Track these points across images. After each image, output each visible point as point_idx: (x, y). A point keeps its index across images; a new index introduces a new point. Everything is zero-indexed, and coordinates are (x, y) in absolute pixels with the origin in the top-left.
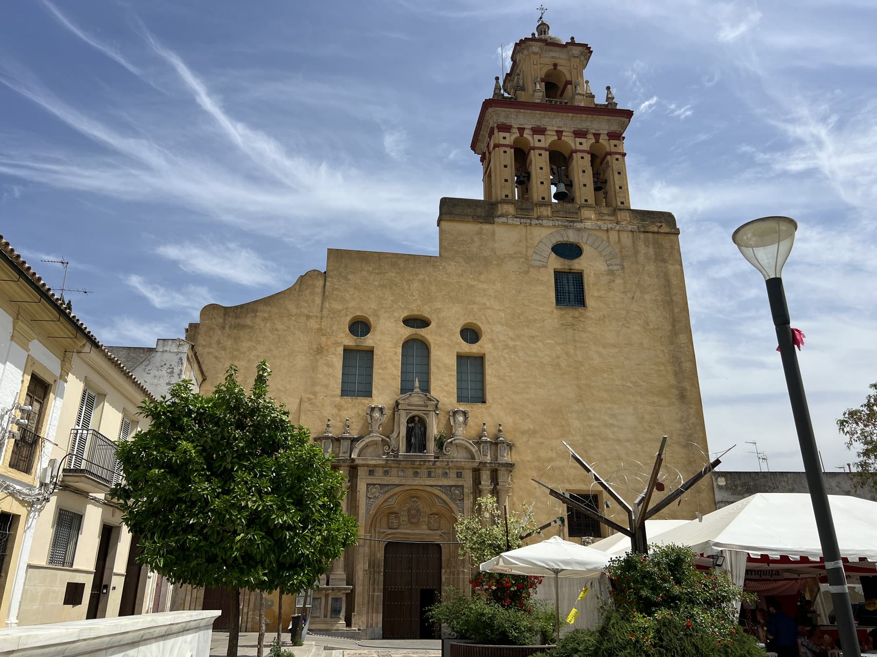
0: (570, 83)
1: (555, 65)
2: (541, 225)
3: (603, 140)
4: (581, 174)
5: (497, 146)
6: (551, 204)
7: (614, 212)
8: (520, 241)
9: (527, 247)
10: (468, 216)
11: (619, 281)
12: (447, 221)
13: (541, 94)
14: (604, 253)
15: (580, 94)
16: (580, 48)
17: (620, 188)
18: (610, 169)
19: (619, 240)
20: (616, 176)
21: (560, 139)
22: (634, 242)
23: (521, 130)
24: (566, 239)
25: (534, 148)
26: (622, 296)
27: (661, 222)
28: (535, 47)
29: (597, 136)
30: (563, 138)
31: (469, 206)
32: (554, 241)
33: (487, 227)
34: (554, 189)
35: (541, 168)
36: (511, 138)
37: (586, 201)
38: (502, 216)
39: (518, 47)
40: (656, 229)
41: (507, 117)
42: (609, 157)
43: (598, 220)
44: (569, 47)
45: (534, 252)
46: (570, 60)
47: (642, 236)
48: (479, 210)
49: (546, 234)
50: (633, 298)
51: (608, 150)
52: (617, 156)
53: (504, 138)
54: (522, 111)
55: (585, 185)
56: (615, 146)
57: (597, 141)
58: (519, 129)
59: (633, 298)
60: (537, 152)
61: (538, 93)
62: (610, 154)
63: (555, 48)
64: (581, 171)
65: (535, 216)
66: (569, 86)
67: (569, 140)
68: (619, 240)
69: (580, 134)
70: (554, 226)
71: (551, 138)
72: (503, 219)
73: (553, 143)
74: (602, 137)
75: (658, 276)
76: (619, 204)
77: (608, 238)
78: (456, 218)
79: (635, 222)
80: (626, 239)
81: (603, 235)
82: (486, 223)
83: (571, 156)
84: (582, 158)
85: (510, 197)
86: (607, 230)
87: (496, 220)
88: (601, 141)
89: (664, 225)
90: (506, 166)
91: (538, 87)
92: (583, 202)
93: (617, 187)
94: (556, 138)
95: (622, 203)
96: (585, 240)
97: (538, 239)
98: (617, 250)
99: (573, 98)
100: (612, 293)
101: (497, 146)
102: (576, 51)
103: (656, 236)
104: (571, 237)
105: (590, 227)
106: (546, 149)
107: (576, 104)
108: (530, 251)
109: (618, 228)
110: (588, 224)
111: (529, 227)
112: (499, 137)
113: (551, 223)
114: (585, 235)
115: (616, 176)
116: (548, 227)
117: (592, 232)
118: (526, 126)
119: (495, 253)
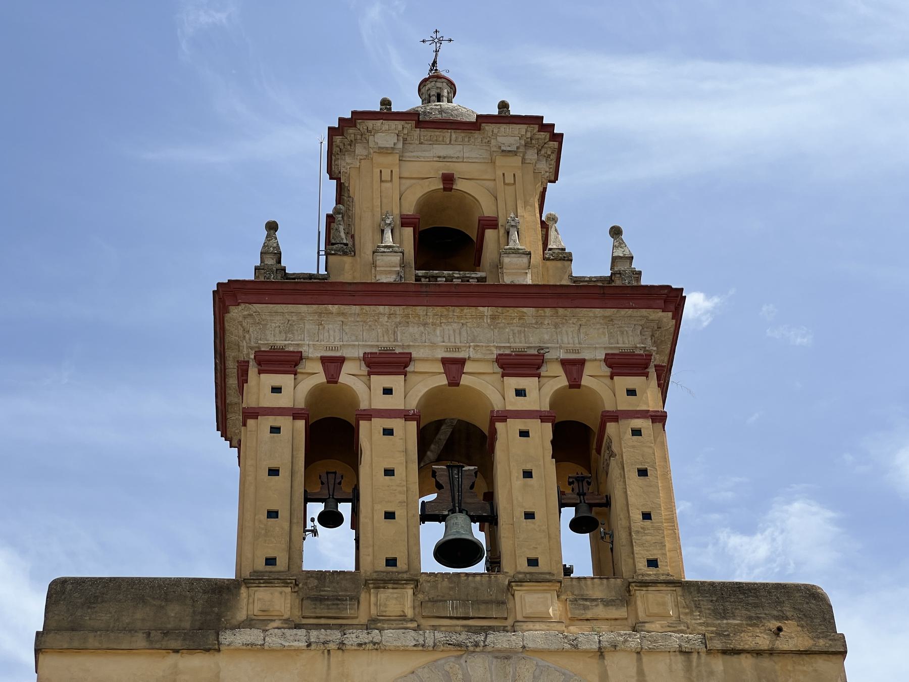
0: (492, 223)
1: (448, 180)
3: (595, 379)
4: (518, 481)
5: (252, 413)
6: (415, 580)
7: (625, 598)
10: (131, 630)
12: (61, 651)
13: (396, 259)
15: (516, 252)
16: (522, 129)
17: (647, 516)
18: (613, 462)
21: (454, 382)
23: (332, 365)
25: (369, 415)
27: (783, 618)
29: (574, 367)
30: (465, 380)
31: (141, 600)
34: (432, 534)
35: (389, 472)
36: (295, 390)
37: (533, 562)
38: (249, 623)
39: (338, 139)
40: (763, 641)
41: (289, 329)
42: (611, 428)
43: (572, 619)
44: (488, 128)
46: (493, 162)
47: (718, 664)
48: (173, 610)
51: (609, 407)
52: (637, 423)
53: (276, 390)
55: (529, 516)
56: (631, 392)
57: (575, 384)
58: (324, 360)
60: (379, 424)
61: (389, 255)
62: (615, 417)
63: (447, 134)
64: (517, 474)
65: (363, 619)
66: (489, 234)
67: (488, 388)
70: (422, 647)
71: (425, 380)
72: (252, 635)
73: (432, 397)
74: (588, 370)
76: (642, 566)
78: (92, 642)
79: (696, 620)
81: (588, 669)
82: (191, 650)
83: (493, 432)
84: (524, 434)
85: (282, 564)
86: (601, 653)
87: (227, 637)
88: (586, 381)
89: (790, 627)
90: (274, 472)
91: (388, 239)
92: (523, 566)
93: (637, 516)
94: (443, 381)
95: (653, 563)
99: (498, 266)
101: (252, 413)
102: (508, 137)
103: (766, 663)
105: (540, 644)
106: (407, 416)
107: (507, 280)
109: (634, 642)
110: (534, 636)
111: (336, 657)
112: (260, 388)
113: (410, 638)
115: (634, 482)
116: (405, 650)
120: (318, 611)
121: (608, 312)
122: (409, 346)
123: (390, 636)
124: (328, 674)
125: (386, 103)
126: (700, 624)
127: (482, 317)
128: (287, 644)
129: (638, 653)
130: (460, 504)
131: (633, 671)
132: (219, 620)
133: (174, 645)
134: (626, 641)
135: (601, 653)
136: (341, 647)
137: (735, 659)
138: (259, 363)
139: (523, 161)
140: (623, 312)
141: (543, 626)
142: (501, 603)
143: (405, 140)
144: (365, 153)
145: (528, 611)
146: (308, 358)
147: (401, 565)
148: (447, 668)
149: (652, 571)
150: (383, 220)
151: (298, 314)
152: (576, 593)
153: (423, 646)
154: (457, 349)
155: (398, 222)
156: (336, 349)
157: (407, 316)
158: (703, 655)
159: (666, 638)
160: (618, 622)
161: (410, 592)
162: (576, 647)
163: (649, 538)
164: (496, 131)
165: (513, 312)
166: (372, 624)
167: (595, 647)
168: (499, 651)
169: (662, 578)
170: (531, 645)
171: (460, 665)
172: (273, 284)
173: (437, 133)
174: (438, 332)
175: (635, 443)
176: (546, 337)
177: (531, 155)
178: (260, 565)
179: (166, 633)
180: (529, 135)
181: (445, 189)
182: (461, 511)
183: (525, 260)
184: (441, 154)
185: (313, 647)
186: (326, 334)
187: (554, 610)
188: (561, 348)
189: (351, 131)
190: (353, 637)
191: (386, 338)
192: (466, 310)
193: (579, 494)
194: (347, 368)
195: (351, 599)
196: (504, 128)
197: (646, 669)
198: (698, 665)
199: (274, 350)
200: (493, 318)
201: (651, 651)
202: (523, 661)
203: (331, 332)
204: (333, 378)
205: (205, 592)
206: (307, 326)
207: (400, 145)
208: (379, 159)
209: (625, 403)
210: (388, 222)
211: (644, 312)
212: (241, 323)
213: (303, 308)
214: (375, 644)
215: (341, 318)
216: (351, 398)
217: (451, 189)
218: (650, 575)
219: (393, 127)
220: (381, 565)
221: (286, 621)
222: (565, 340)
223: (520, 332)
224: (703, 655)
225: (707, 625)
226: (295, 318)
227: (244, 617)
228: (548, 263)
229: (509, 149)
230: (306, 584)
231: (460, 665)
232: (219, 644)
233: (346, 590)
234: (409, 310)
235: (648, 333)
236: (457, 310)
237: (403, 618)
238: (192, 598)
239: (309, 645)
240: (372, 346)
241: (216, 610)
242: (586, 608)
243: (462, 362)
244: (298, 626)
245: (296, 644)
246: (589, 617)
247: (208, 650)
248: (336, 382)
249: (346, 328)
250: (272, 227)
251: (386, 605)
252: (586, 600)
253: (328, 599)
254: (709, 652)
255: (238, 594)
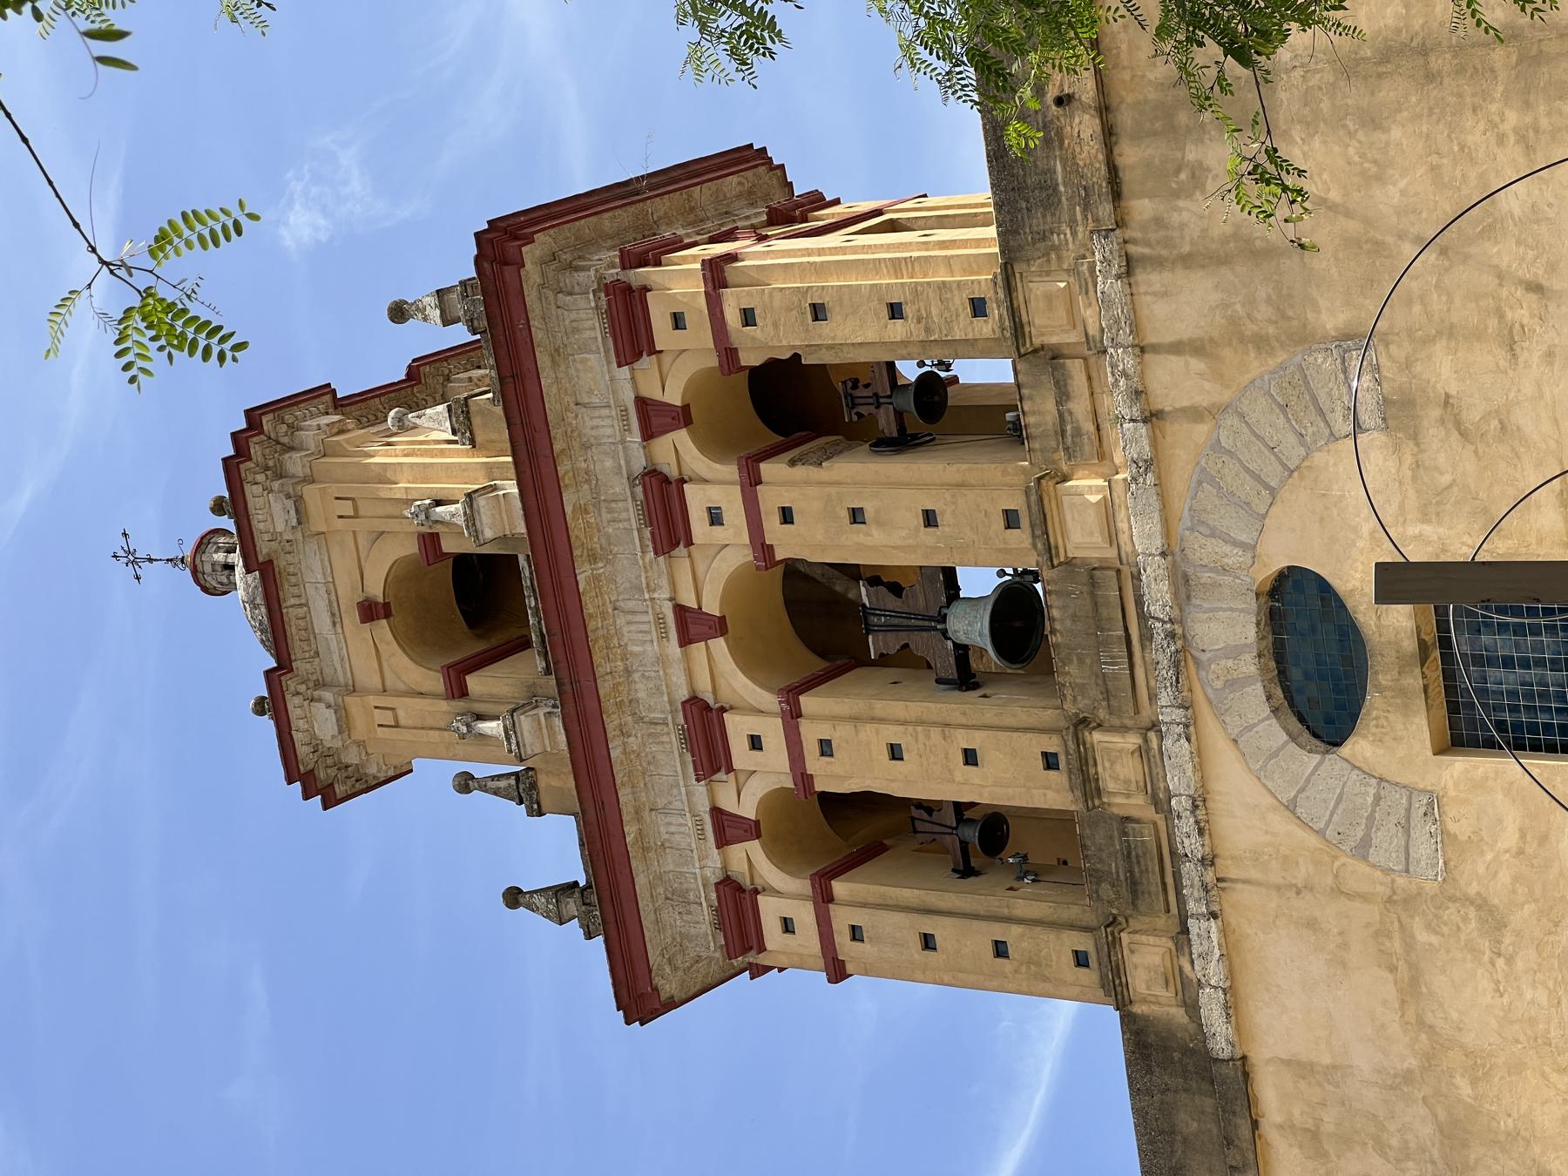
0: (430, 541)
1: (370, 611)
2: (1199, 802)
8: (1312, 924)
9: (1338, 891)
11: (1442, 370)
14: (1294, 453)
17: (895, 311)
19: (1194, 348)
20: (827, 332)
22: (1187, 261)
24: (1248, 665)
26: (1531, 354)
28: (317, 722)
30: (712, 607)
32: (1273, 733)
33: (1270, 1093)
37: (1011, 519)
38: (1192, 1008)
40: (1084, 126)
41: (681, 898)
43: (1102, 455)
44: (264, 549)
45: (1362, 849)
47: (1141, 208)
49: (1242, 779)
50: (1536, 288)
51: (713, 361)
52: (732, 317)
54: (631, 831)
57: (682, 417)
59: (1536, 288)
63: (291, 614)
67: (717, 564)
68: (1194, 348)
69: (665, 512)
70: (1189, 729)
73: (749, 661)
75: (1373, 121)
77: (1195, 414)
80: (1180, 305)
81: (1186, 442)
85: (1085, 943)
86: (1152, 417)
87: (1220, 1045)
92: (1020, 538)
95: (978, 308)
96: (1234, 557)
97: (1281, 823)
98: (1256, 366)
100: (1523, 419)
103: (1125, 119)
104: (1230, 631)
105: (1154, 525)
107: (521, 528)
108: (1358, 874)
110: (1141, 535)
111: (1227, 868)
113: (1177, 749)
114: (1203, 550)
116: (1200, 758)
117: (1181, 505)
118: (704, 808)
119: (1408, 1077)
120: (1153, 889)
121: (543, 360)
122: (671, 702)
123: (1179, 780)
124: (1258, 884)
125: (260, 707)
126: (1074, 234)
127: (596, 578)
128: (1217, 953)
129: (1143, 350)
130: (931, 619)
131: (1175, 362)
132: (1193, 1052)
133: (1245, 1130)
134: (1124, 374)
135: (1152, 417)
136: (1208, 861)
137: (1126, 177)
138: (746, 950)
139: (310, 480)
140: (538, 336)
141: (1121, 515)
142: (1093, 583)
143: (319, 685)
144: (354, 750)
145: (1098, 539)
146: (725, 868)
147: (1053, 744)
148: (1219, 684)
149: (994, 311)
150: (463, 737)
151: (652, 886)
152: (1053, 444)
153: (1187, 726)
154: (660, 620)
155: (460, 705)
156: (699, 823)
157: (619, 705)
158: (1129, 234)
159: (1106, 302)
160: (1094, 374)
161: (1097, 736)
162: (1149, 464)
163: (934, 312)
164: (266, 537)
165: (576, 527)
166: (1160, 801)
167: (1143, 429)
168: (1176, 595)
169: (1001, 295)
170: (1158, 543)
171: (1210, 661)
172: (604, 898)
173: (293, 631)
174: (636, 649)
175: (769, 321)
176: (609, 463)
177: (295, 463)
178: (1089, 976)
179: (1229, 1142)
180: (260, 478)
181: (387, 615)
182: (943, 619)
183: (481, 502)
184: (328, 620)
185: (1215, 908)
186: (677, 837)
187: (1087, 486)
188: (623, 442)
189: (322, 775)
190: (1191, 844)
191: (665, 739)
192: (590, 609)
193: (878, 406)
194: (728, 803)
195: (1125, 834)
196: (259, 524)
197: (1169, 338)
198: (1148, 244)
199: (721, 924)
200: (593, 558)
201: (1135, 329)
202: (1187, 551)
203: (672, 829)
204: (752, 830)
205: (1150, 1071)
206: (671, 867)
207: (328, 695)
208: (360, 731)
209: (700, 335)
210: (464, 729)
211: (531, 297)
212: (687, 970)
213: (641, 881)
214: (1195, 807)
215: (646, 814)
216: (775, 801)
217: (386, 605)
218: (1000, 316)
219: (298, 711)
220: (1057, 778)
221: (1179, 948)
222: (609, 431)
223: (610, 511)
224: (1129, 234)
225: (1072, 223)
226: (661, 890)
227: (1182, 1011)
228: (478, 439)
229: (293, 512)
230: (1110, 903)
231: (1210, 661)
232: (1232, 1059)
233: (1111, 837)
234: (608, 705)
235: (569, 279)
236: (591, 625)
237: (1143, 752)
238: (1163, 1092)
239: (1214, 915)
240: (683, 763)
241: (1176, 1055)
242: (1078, 432)
243: (681, 611)
244: (1185, 931)
245: (1214, 936)
246: (1092, 428)
247: (1246, 1075)
248: (757, 823)
249: (661, 802)
250: (514, 897)
251: (1127, 782)
252: (1063, 432)
253: (1131, 872)
254: (1120, 223)
255: (1145, 1018)
